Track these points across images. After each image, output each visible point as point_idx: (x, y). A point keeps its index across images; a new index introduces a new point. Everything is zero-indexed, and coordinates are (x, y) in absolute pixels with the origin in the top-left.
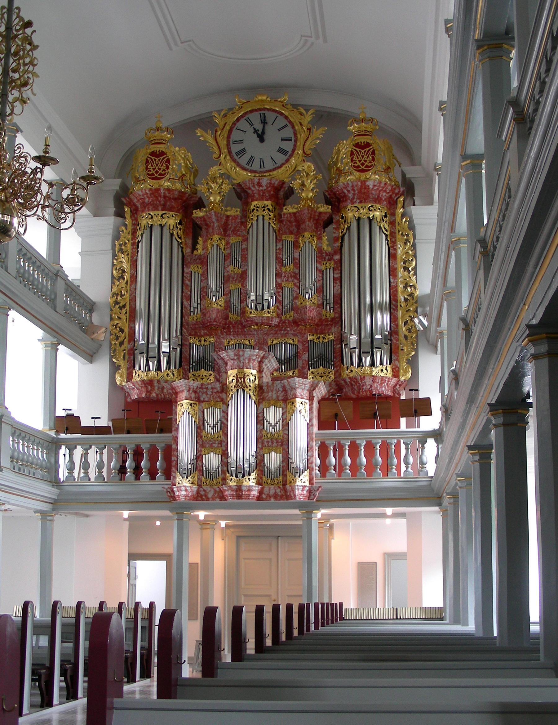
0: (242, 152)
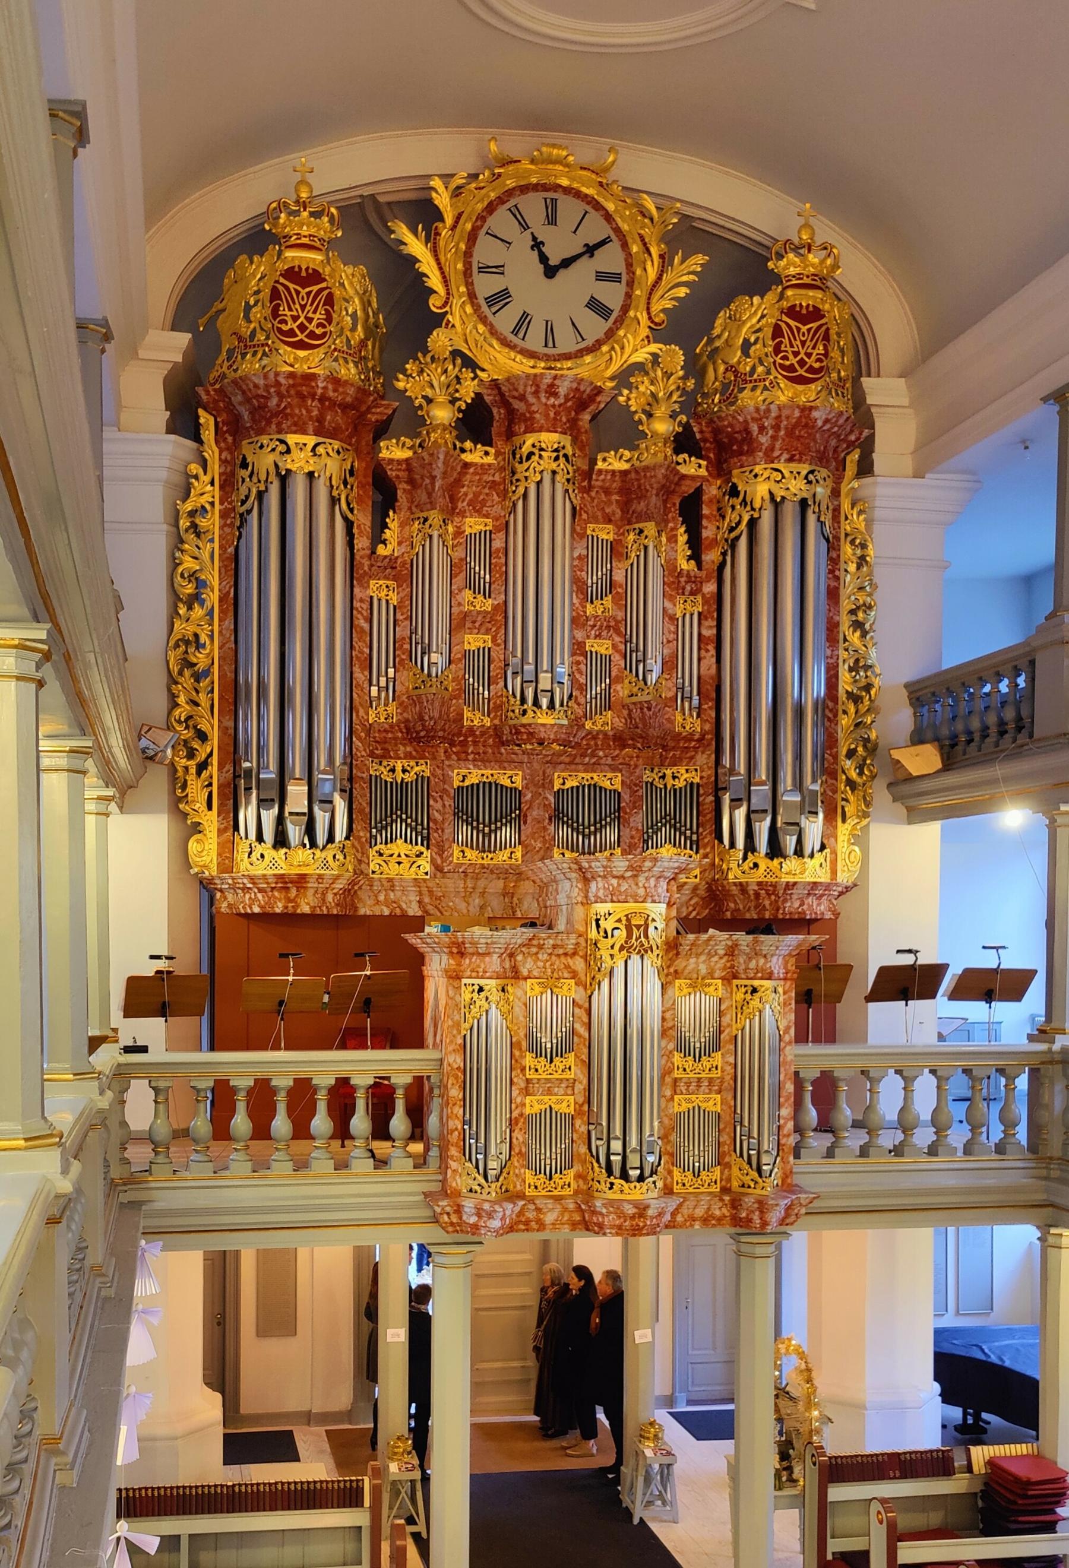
0: (501, 298)
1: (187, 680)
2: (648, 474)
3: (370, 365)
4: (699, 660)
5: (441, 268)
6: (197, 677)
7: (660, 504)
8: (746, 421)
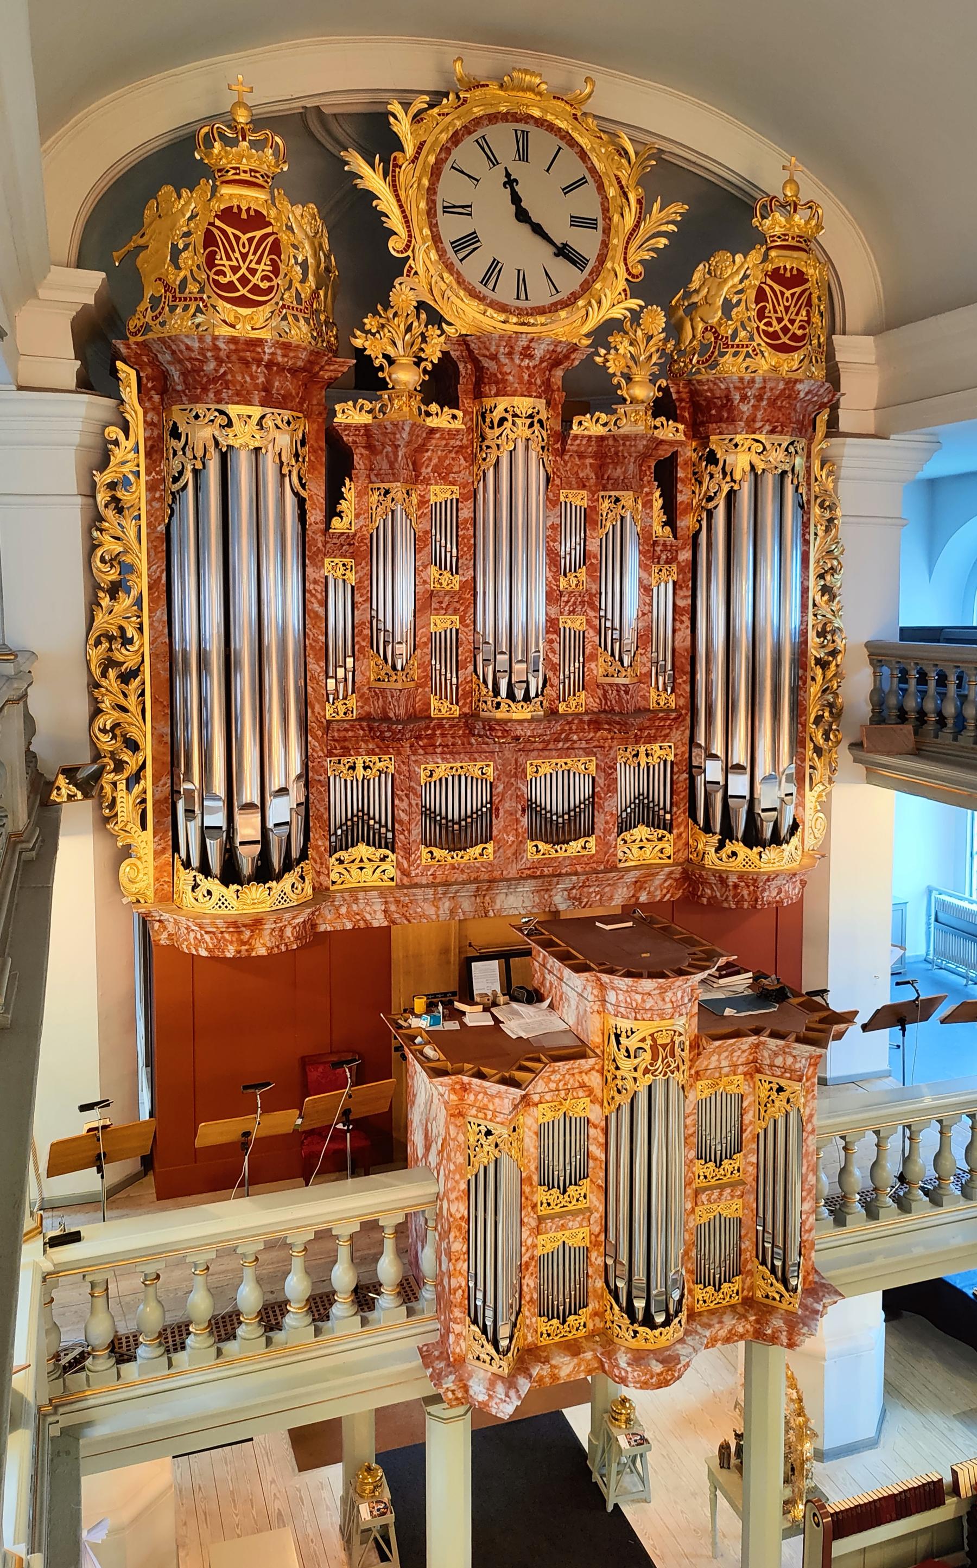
0: (468, 243)
1: (112, 680)
2: (628, 443)
3: (322, 318)
4: (674, 631)
5: (401, 206)
6: (126, 678)
7: (637, 471)
8: (728, 389)
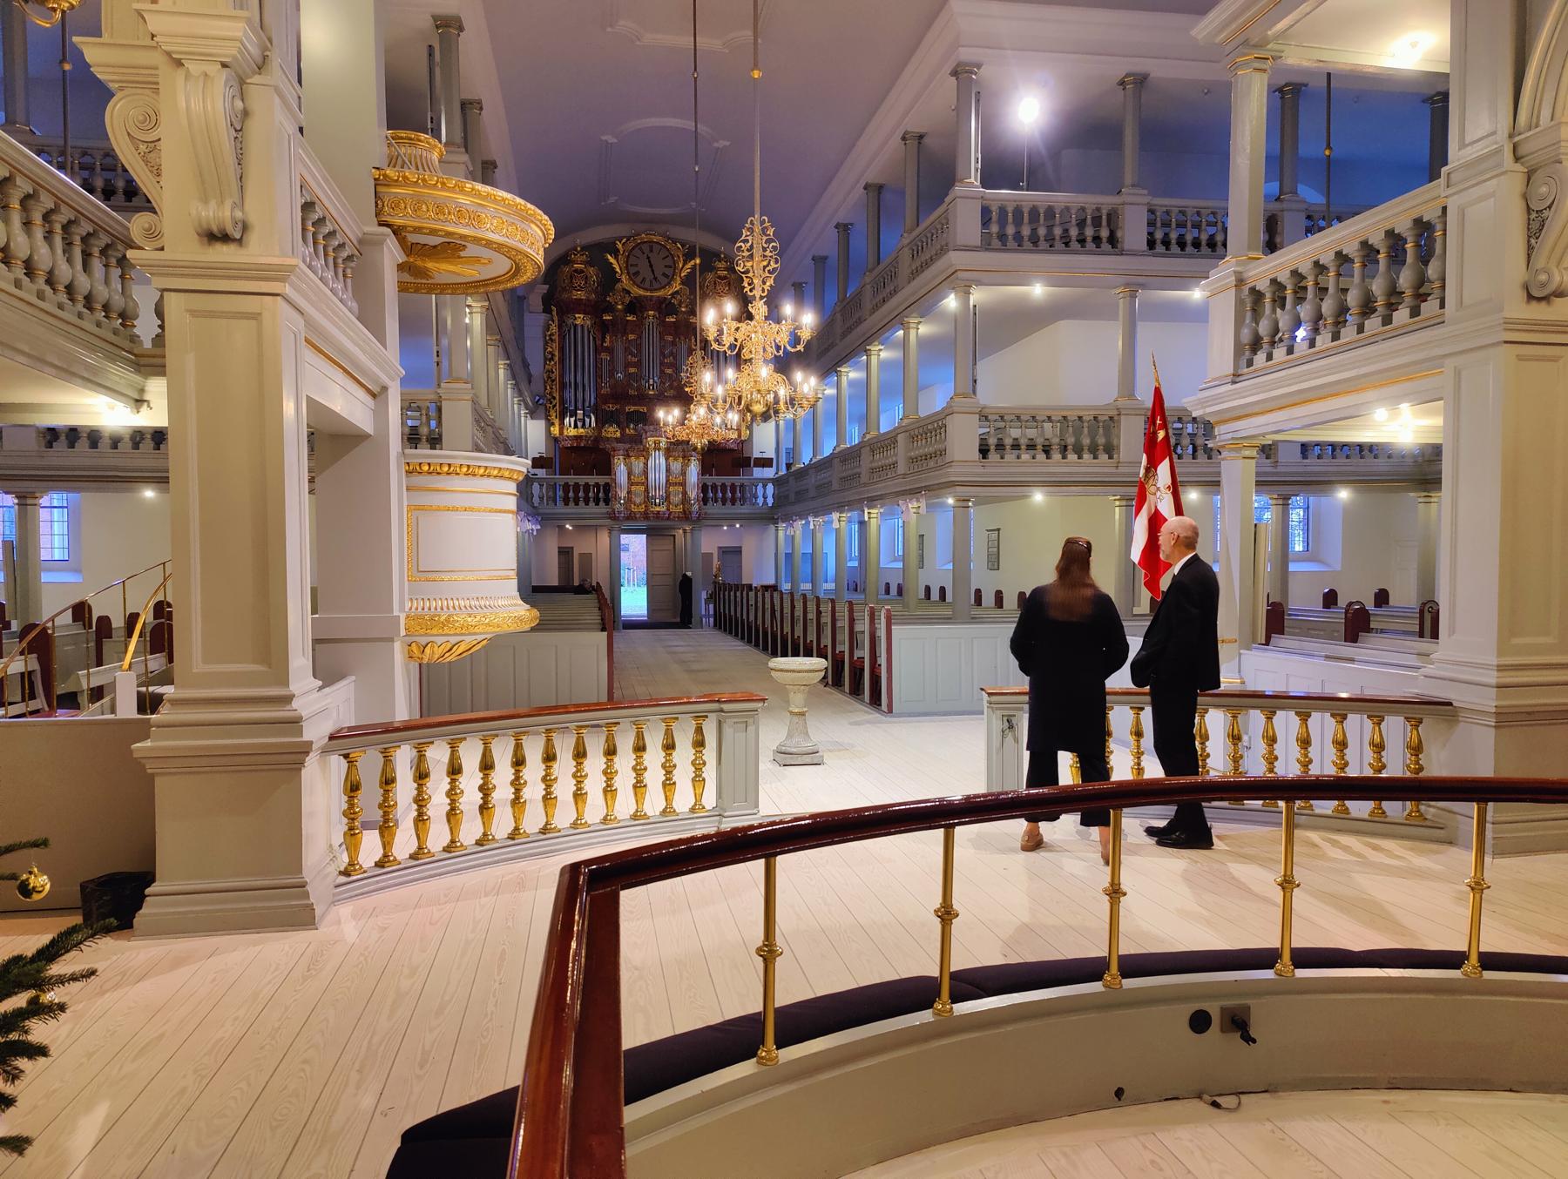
0: (637, 273)
